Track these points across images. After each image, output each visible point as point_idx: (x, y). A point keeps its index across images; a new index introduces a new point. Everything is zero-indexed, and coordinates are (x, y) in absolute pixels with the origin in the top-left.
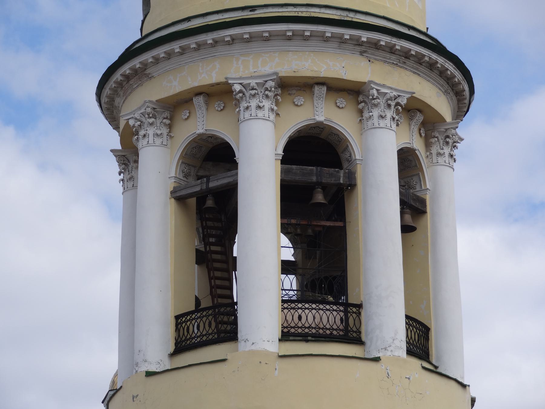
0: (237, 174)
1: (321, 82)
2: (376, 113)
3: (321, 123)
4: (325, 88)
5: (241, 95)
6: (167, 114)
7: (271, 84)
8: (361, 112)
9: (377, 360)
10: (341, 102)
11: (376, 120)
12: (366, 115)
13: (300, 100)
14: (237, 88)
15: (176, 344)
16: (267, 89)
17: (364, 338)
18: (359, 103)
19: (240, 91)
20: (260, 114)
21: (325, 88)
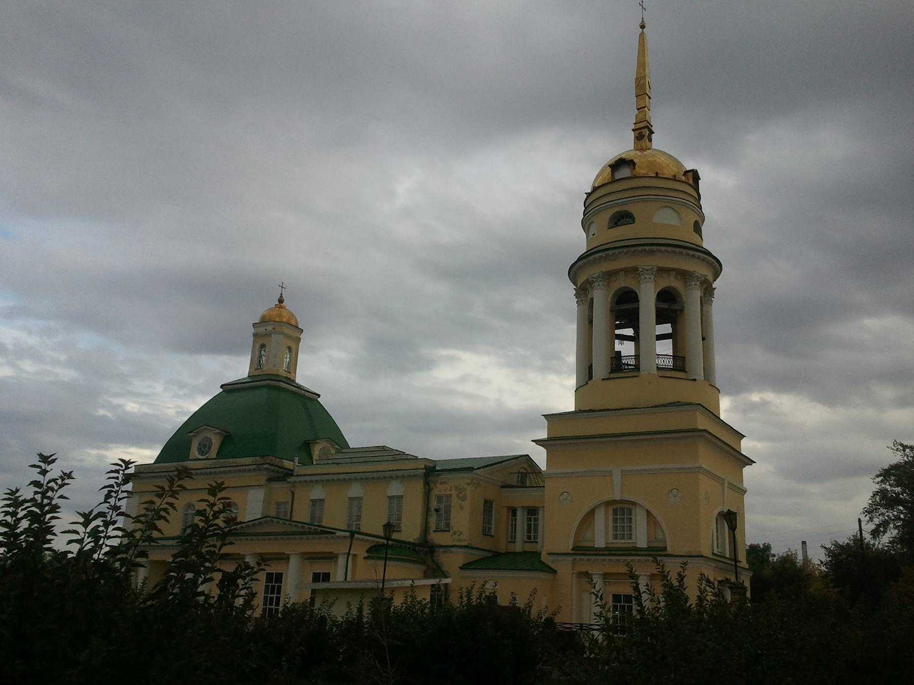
0: (639, 304)
1: (674, 270)
2: (693, 283)
3: (672, 286)
5: (642, 273)
6: (608, 277)
8: (686, 282)
9: (695, 380)
10: (679, 277)
11: (693, 286)
14: (641, 269)
17: (686, 370)
18: (686, 279)
19: (642, 271)
20: (650, 280)
21: (674, 273)
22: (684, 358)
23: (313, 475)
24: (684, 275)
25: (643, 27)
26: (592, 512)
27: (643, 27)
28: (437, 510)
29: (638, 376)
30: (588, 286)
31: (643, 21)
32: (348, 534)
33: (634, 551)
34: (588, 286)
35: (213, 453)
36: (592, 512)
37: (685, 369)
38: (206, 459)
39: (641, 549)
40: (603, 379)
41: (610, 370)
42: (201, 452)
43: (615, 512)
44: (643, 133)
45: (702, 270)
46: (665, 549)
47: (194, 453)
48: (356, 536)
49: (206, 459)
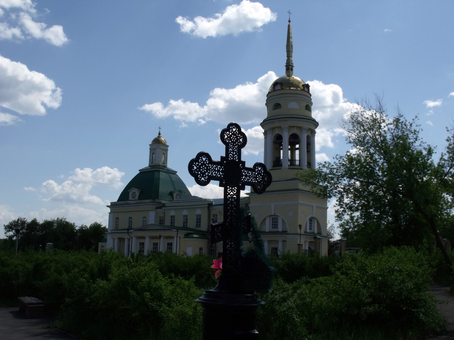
23: (175, 206)
25: (289, 21)
26: (265, 219)
27: (289, 21)
28: (213, 219)
31: (289, 19)
32: (176, 230)
33: (277, 233)
35: (137, 198)
36: (265, 219)
38: (134, 200)
39: (267, 232)
42: (133, 198)
43: (273, 219)
44: (289, 67)
46: (287, 232)
47: (130, 198)
48: (179, 231)
49: (134, 200)
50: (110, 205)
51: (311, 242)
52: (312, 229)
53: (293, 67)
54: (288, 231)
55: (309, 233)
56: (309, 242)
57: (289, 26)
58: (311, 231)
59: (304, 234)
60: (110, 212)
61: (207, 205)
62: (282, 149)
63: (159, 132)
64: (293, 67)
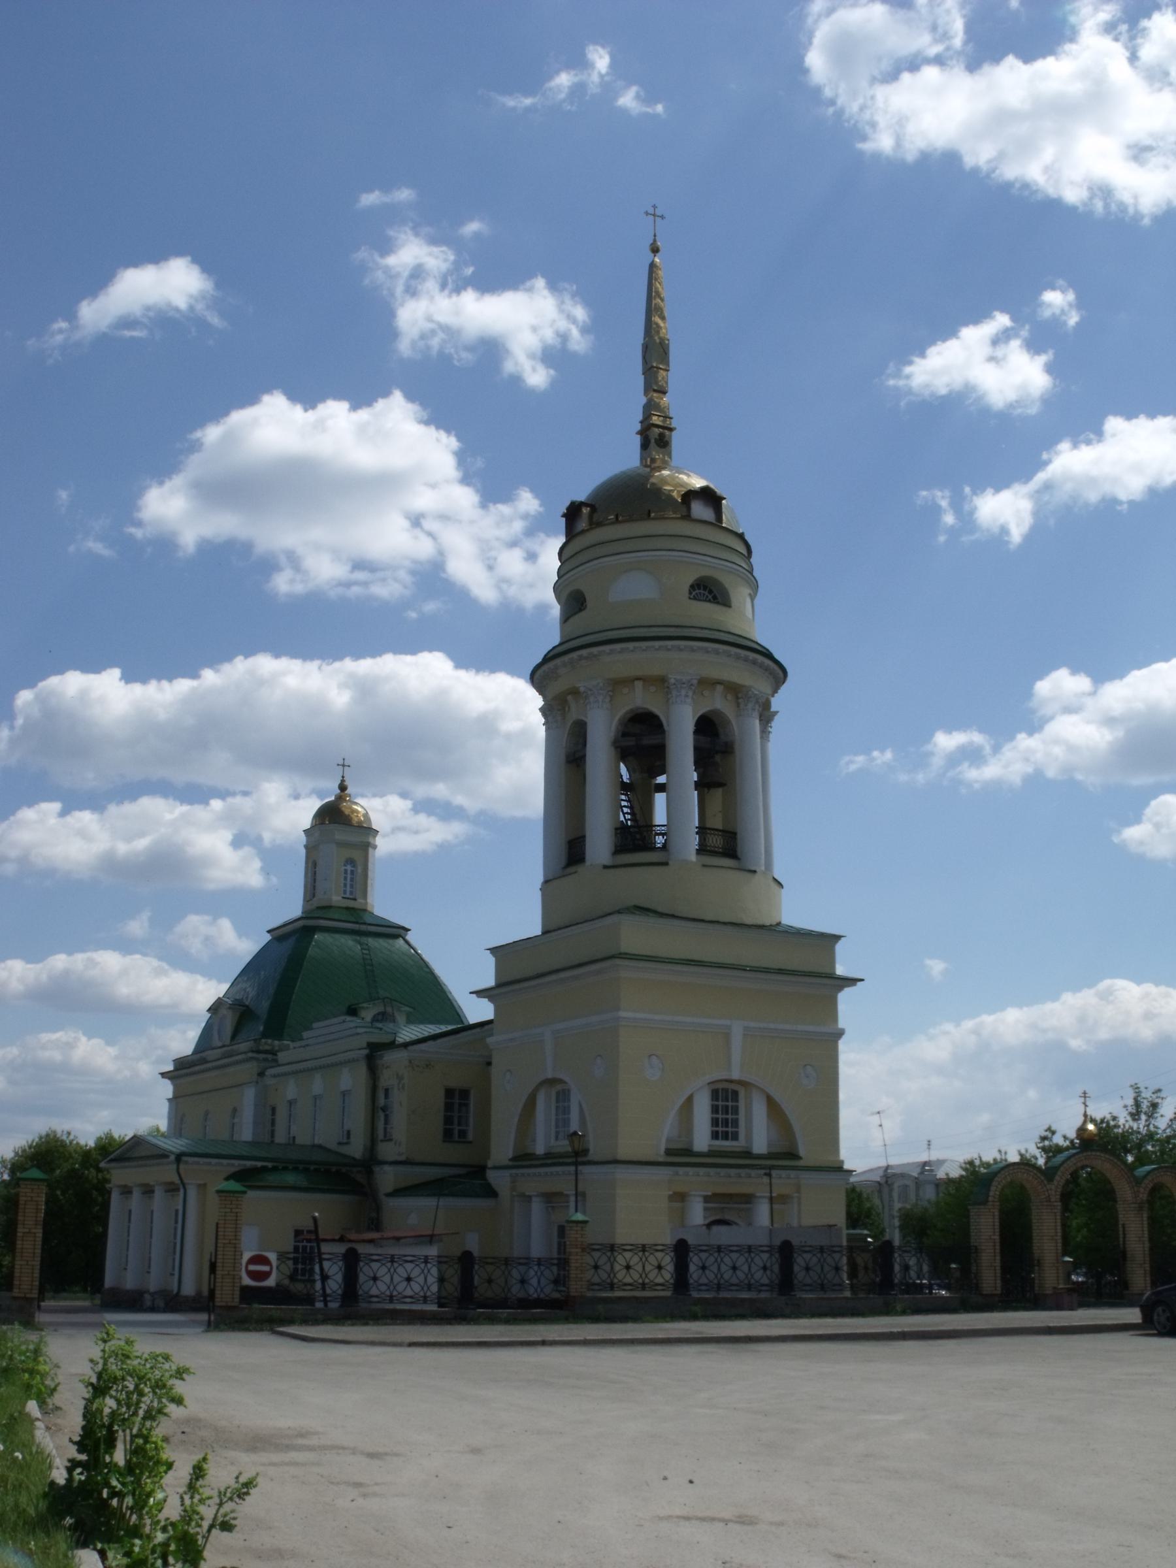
1: (719, 682)
2: (750, 706)
4: (722, 687)
7: (695, 682)
8: (738, 705)
10: (729, 697)
12: (742, 706)
13: (706, 693)
15: (616, 846)
16: (692, 685)
22: (735, 834)
24: (736, 691)
25: (655, 250)
29: (666, 864)
30: (569, 698)
31: (655, 241)
34: (569, 698)
37: (735, 851)
40: (605, 867)
41: (613, 849)
45: (760, 685)
50: (170, 1068)
51: (715, 1195)
52: (742, 1136)
53: (671, 430)
54: (591, 1152)
55: (711, 1153)
56: (707, 1199)
57: (652, 266)
58: (734, 1143)
59: (661, 1159)
60: (171, 1096)
61: (366, 1052)
62: (661, 788)
63: (343, 781)
64: (671, 430)
